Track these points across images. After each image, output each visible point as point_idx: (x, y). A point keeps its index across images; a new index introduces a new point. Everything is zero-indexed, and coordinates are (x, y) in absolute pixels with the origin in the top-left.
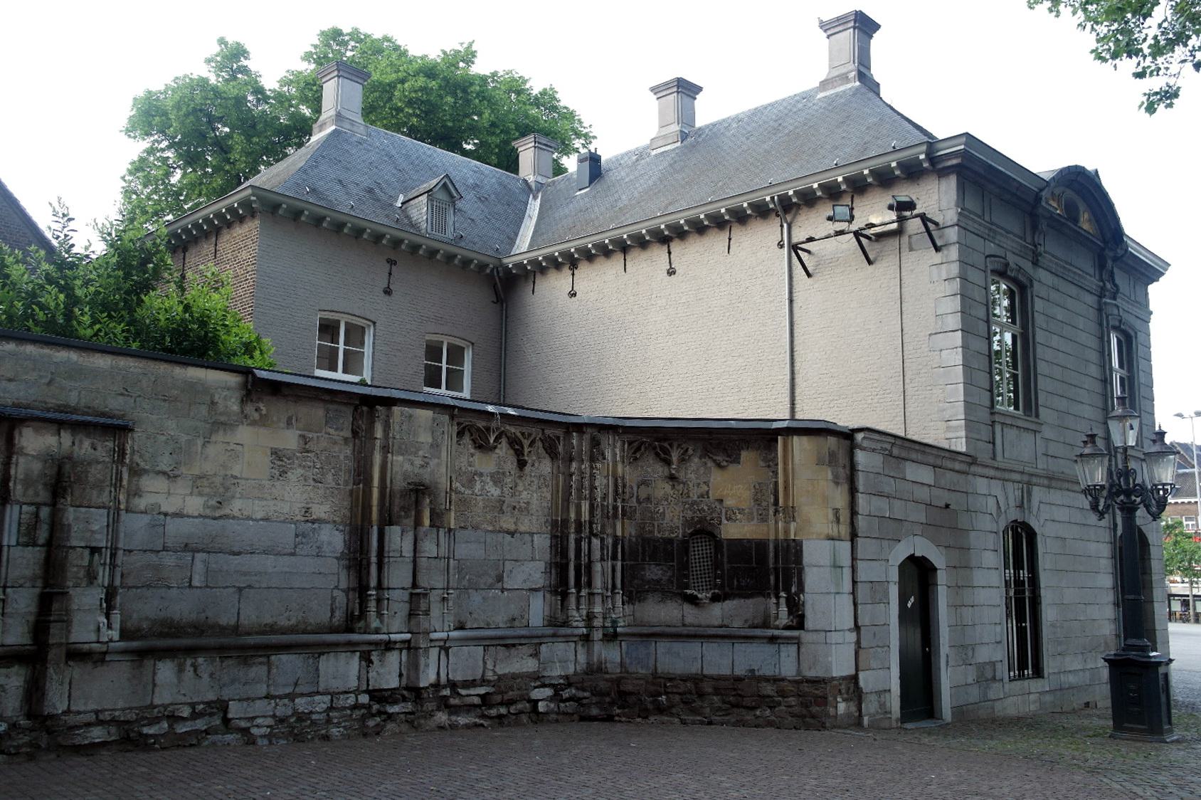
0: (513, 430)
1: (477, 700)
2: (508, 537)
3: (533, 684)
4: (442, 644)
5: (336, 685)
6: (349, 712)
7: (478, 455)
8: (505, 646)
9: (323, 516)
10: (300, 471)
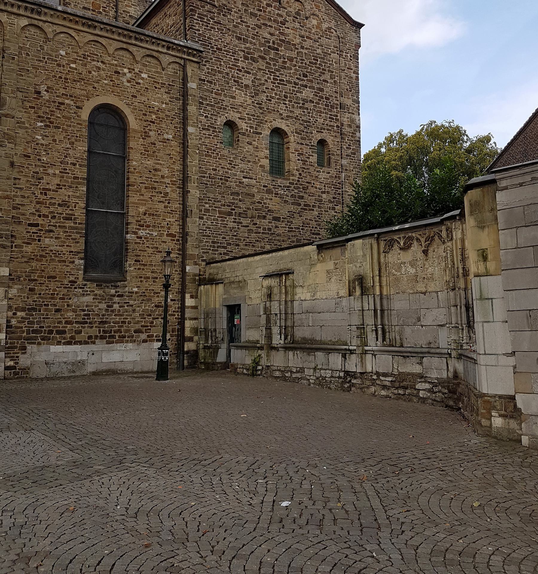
0: (414, 235)
1: (388, 384)
2: (422, 295)
3: (419, 380)
4: (372, 353)
5: (334, 367)
6: (338, 379)
7: (402, 252)
8: (403, 356)
9: (343, 295)
10: (335, 277)
